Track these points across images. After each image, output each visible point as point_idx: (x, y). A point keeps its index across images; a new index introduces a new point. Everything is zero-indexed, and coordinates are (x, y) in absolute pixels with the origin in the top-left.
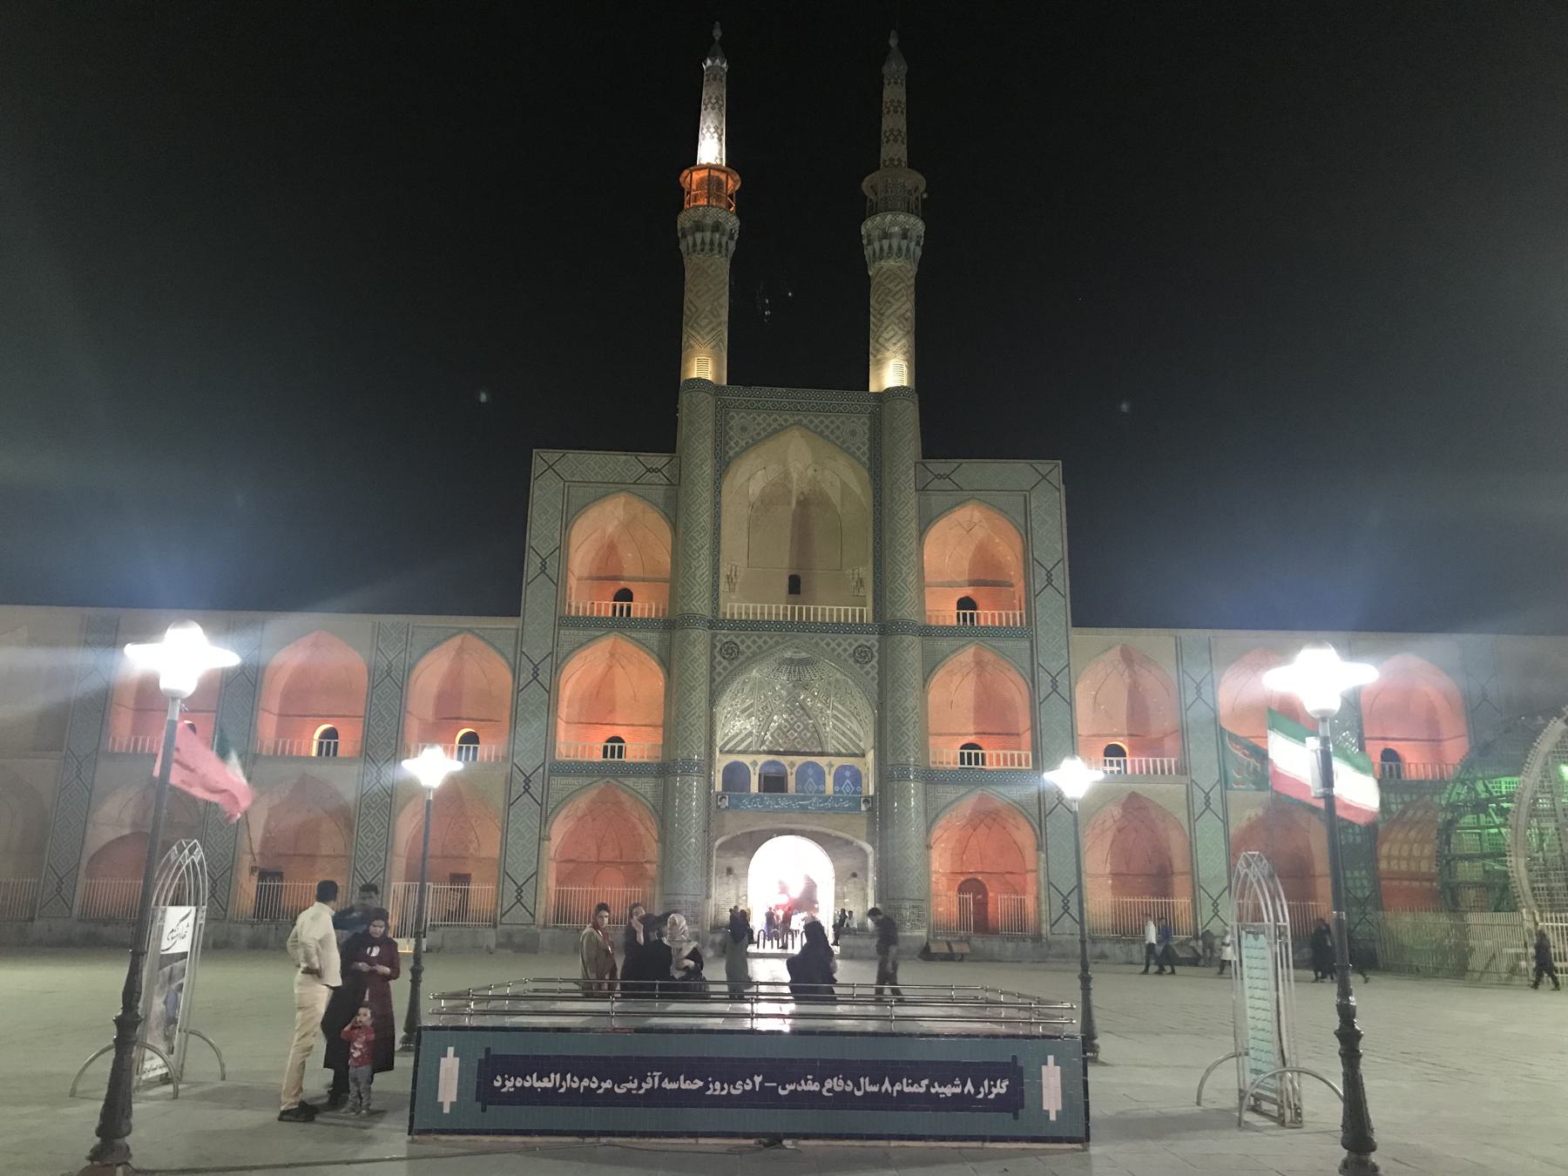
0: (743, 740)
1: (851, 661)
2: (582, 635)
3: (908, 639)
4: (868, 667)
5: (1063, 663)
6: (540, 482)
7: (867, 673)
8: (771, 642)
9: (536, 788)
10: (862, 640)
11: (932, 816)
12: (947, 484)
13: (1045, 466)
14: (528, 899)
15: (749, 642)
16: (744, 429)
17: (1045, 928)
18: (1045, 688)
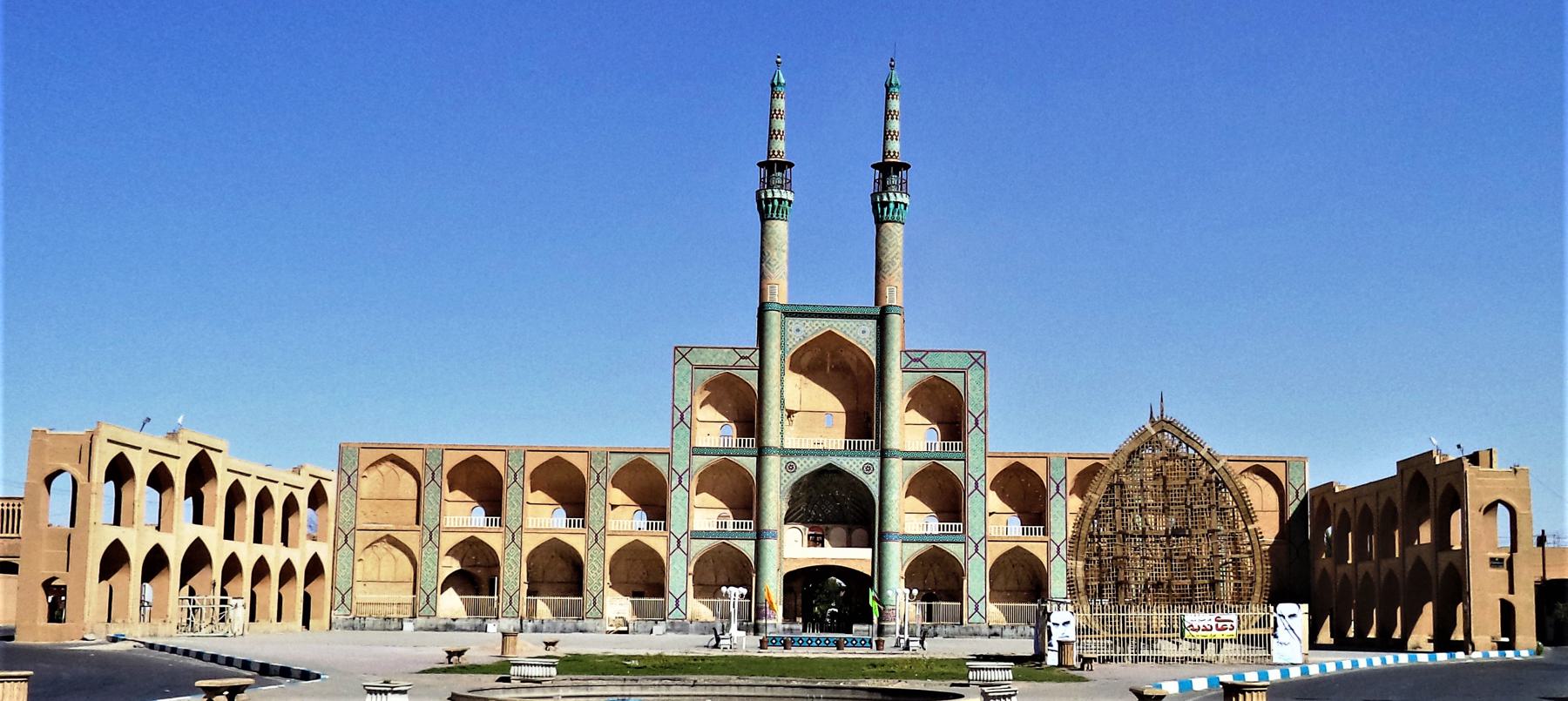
3: (893, 460)
9: (684, 545)
10: (868, 460)
12: (919, 365)
14: (682, 606)
18: (971, 488)
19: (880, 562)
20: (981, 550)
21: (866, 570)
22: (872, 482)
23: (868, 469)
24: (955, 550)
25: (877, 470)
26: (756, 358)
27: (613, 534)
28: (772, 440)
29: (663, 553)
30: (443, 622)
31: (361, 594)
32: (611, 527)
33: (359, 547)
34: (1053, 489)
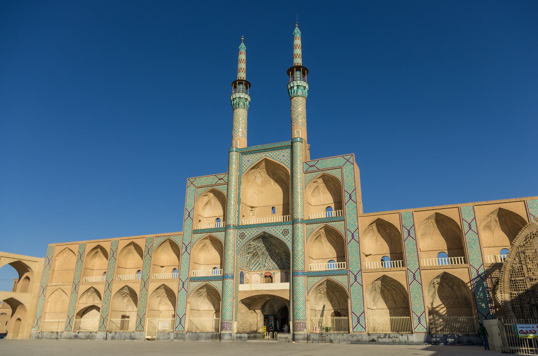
0: (258, 266)
1: (281, 235)
2: (199, 235)
4: (287, 237)
5: (356, 227)
6: (189, 188)
7: (287, 239)
8: (255, 231)
9: (185, 286)
10: (285, 227)
11: (309, 289)
12: (314, 169)
13: (347, 157)
15: (248, 232)
16: (248, 161)
17: (351, 329)
18: (349, 238)
19: (292, 291)
20: (359, 280)
21: (286, 296)
22: (287, 240)
23: (285, 232)
24: (341, 280)
25: (291, 233)
26: (226, 179)
27: (153, 281)
28: (232, 221)
29: (176, 291)
30: (74, 334)
31: (47, 319)
32: (152, 277)
33: (48, 294)
34: (405, 234)
